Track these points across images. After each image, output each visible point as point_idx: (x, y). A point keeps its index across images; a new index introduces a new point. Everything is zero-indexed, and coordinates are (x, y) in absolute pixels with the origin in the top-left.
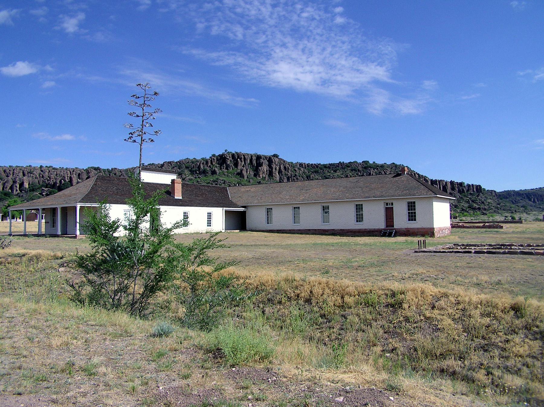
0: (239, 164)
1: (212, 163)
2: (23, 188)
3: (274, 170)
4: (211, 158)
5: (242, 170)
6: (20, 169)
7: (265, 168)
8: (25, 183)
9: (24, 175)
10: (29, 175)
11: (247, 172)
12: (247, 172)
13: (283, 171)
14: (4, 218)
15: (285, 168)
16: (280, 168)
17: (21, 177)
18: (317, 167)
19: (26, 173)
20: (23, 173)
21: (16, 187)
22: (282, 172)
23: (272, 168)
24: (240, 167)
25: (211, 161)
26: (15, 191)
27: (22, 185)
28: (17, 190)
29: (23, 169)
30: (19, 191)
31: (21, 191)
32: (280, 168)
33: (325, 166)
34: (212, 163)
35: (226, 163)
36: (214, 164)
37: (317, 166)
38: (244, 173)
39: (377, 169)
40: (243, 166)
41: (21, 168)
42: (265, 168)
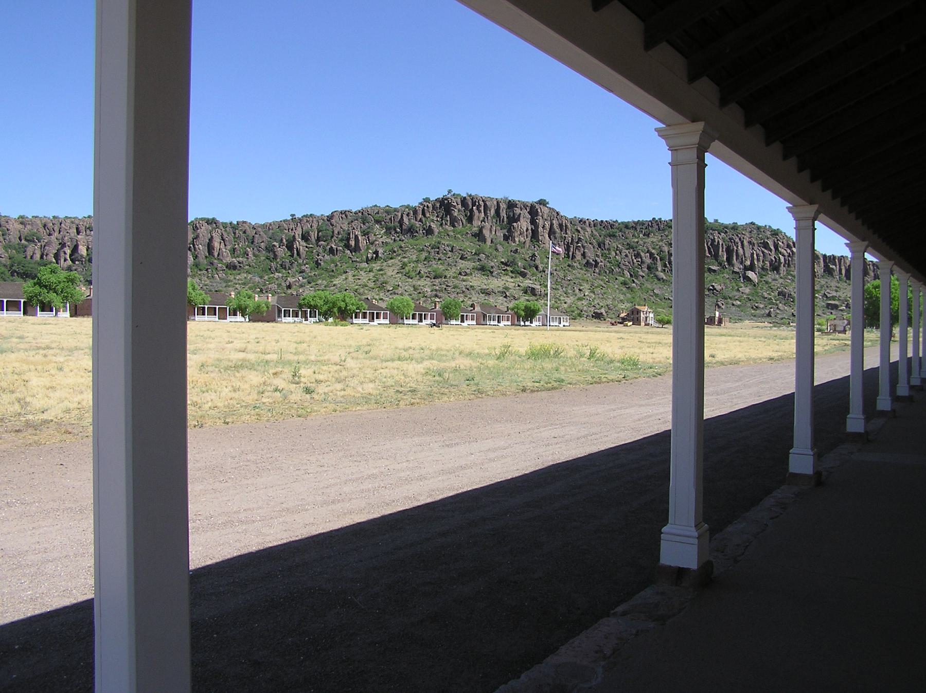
0: (476, 217)
1: (424, 214)
2: (76, 255)
3: (540, 229)
4: (421, 204)
5: (481, 230)
6: (72, 223)
7: (524, 224)
8: (80, 247)
9: (78, 232)
10: (88, 232)
11: (491, 231)
12: (491, 231)
13: (558, 231)
14: (29, 308)
15: (561, 226)
16: (552, 225)
17: (72, 235)
18: (612, 226)
19: (82, 228)
20: (77, 229)
21: (65, 253)
22: (555, 233)
23: (537, 226)
24: (476, 223)
25: (423, 210)
26: (62, 260)
27: (75, 249)
28: (65, 260)
29: (77, 222)
30: (69, 262)
31: (73, 261)
32: (552, 225)
33: (626, 226)
34: (424, 214)
35: (451, 215)
36: (428, 215)
37: (611, 225)
38: (486, 232)
39: (726, 232)
40: (483, 221)
41: (73, 220)
42: (524, 224)
